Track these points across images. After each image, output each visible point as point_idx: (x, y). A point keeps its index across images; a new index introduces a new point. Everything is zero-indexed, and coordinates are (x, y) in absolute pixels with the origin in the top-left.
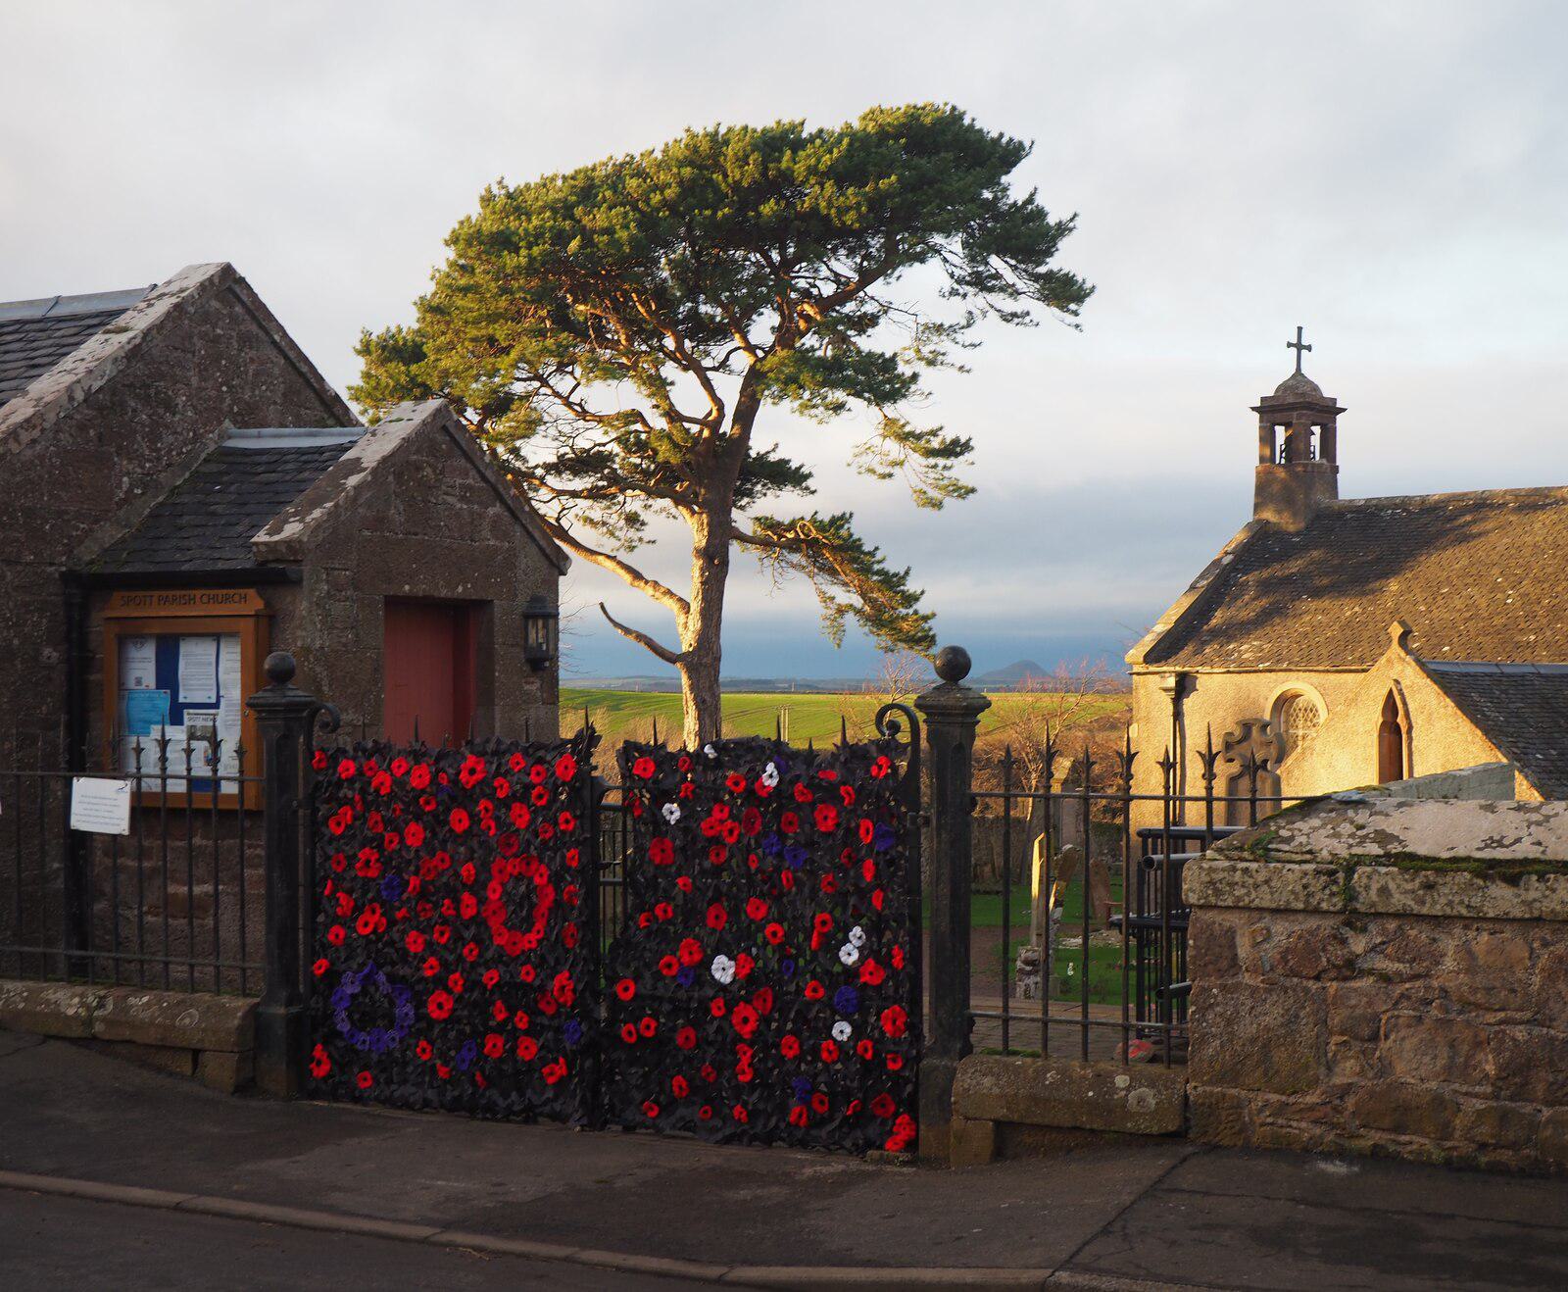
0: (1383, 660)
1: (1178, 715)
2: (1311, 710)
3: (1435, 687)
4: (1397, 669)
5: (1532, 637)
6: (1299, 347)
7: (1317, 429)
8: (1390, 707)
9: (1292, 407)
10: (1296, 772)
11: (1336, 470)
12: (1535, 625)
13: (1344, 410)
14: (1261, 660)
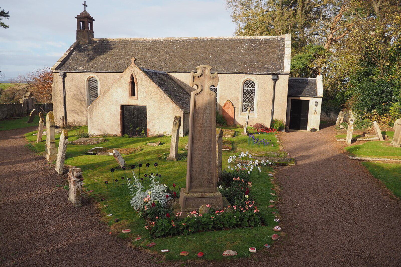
0: (130, 67)
1: (64, 82)
2: (95, 81)
3: (143, 73)
4: (134, 70)
5: (143, 66)
6: (85, 6)
8: (132, 78)
9: (84, 18)
10: (107, 94)
11: (93, 32)
12: (143, 64)
14: (83, 70)
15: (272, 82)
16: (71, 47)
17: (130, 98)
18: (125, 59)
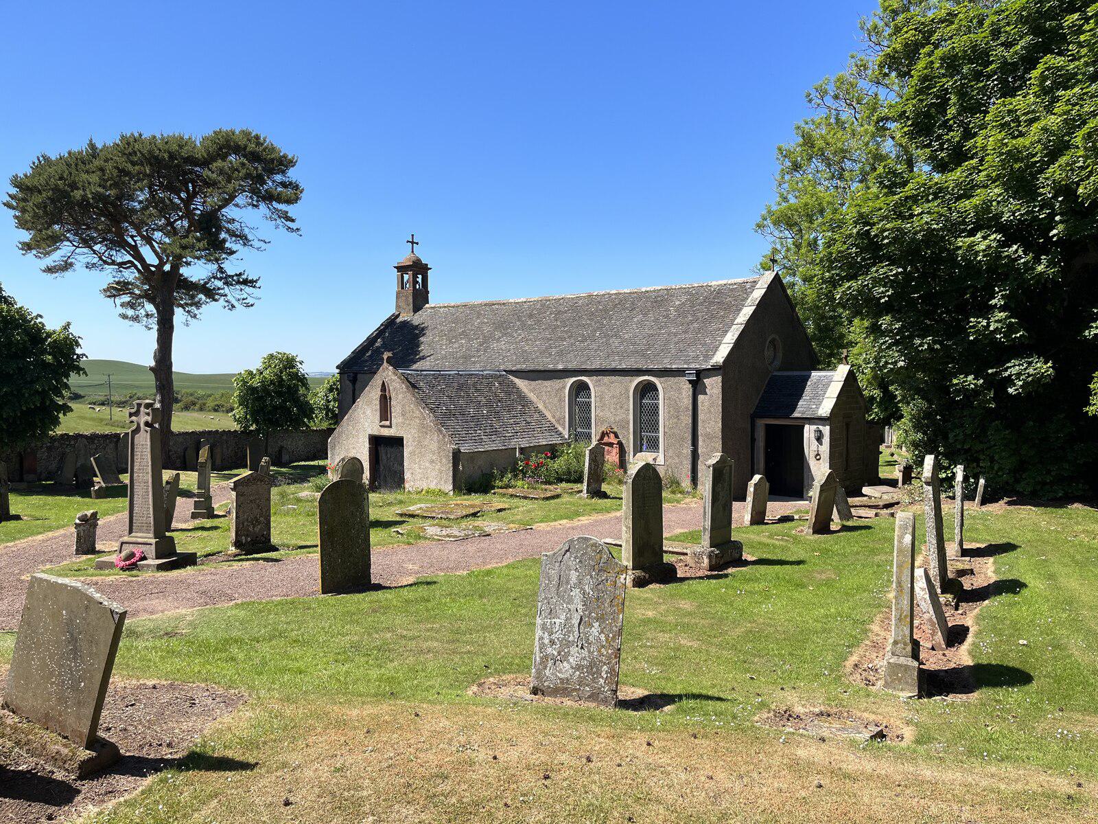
7: (420, 276)
13: (431, 269)
15: (687, 389)
16: (382, 325)
17: (381, 424)
18: (456, 345)
